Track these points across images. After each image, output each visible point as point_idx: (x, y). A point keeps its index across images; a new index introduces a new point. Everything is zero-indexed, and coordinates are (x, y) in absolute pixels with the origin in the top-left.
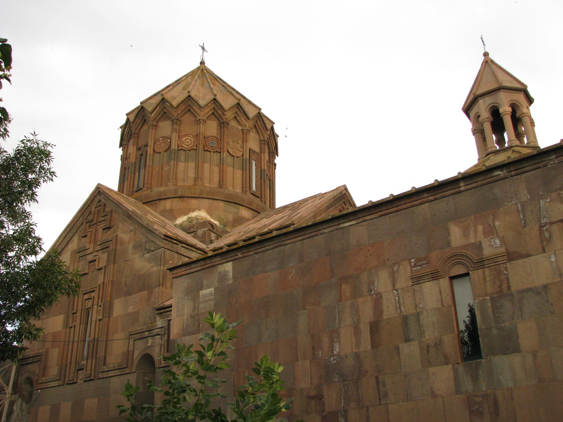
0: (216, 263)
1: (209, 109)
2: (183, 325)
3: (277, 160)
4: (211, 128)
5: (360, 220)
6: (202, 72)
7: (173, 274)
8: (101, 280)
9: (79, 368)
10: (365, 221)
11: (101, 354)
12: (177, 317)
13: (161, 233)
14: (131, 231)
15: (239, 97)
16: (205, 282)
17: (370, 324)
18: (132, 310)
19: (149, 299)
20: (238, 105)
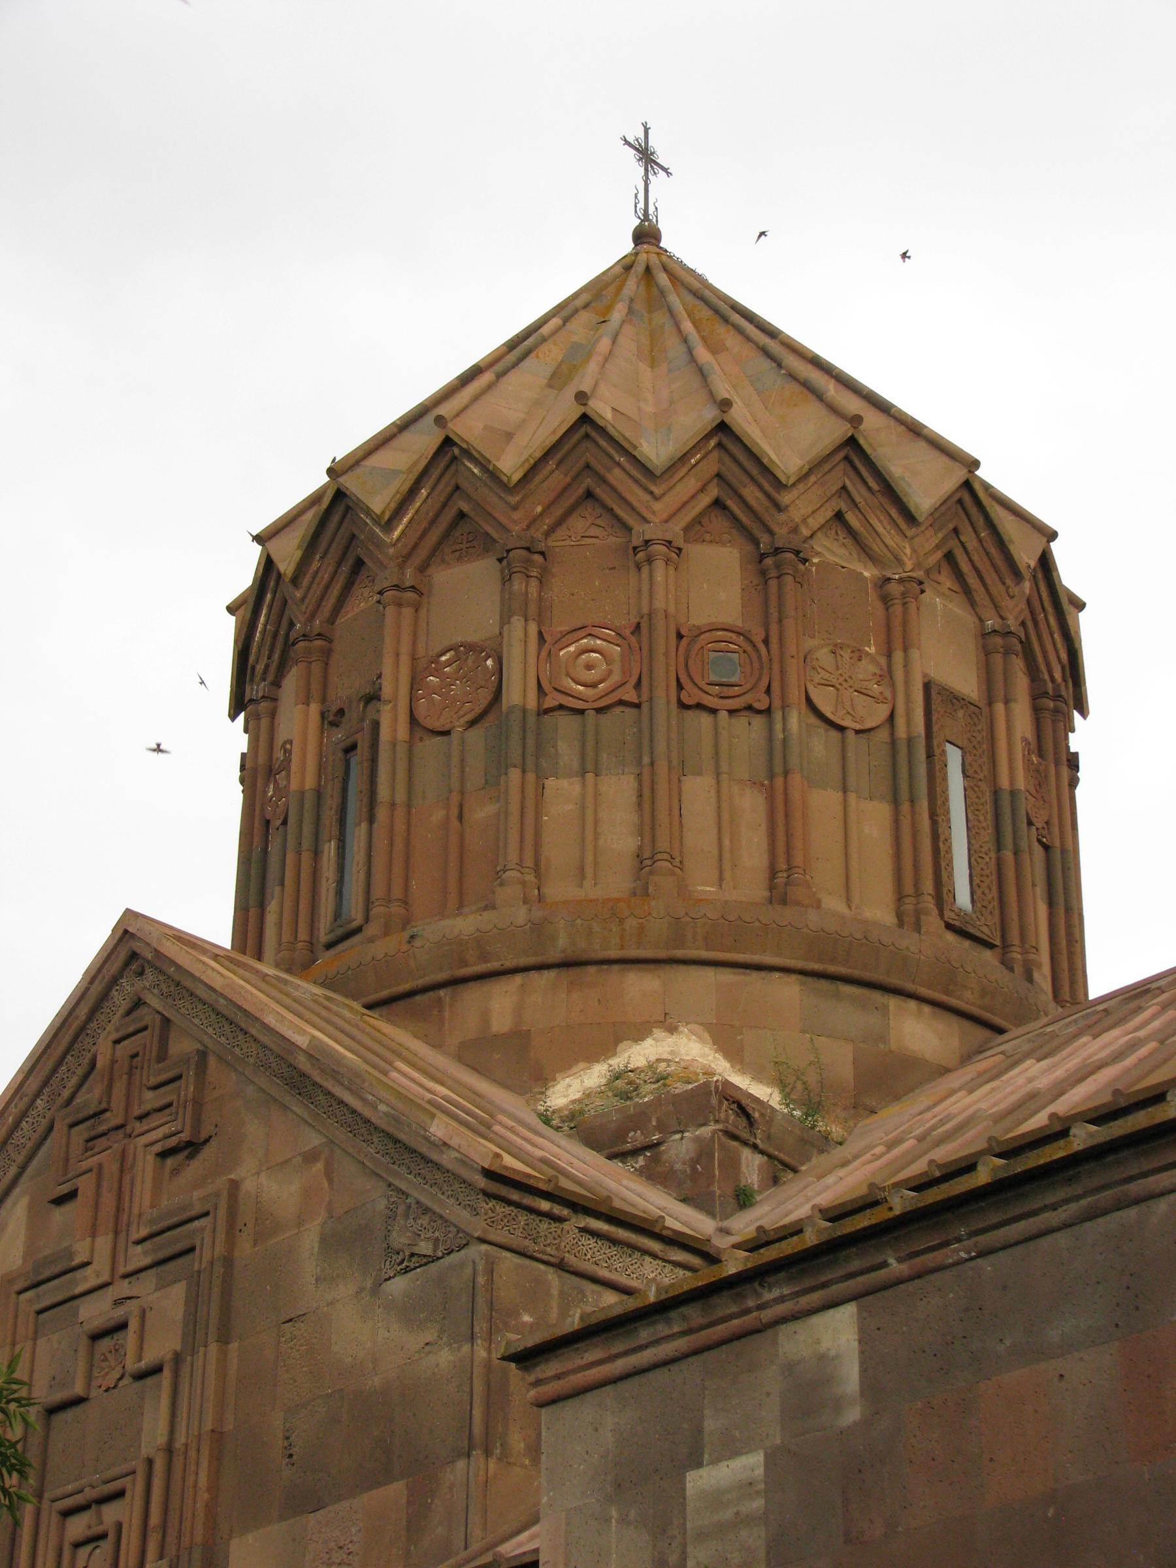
0: (767, 1315)
1: (692, 484)
3: (1083, 737)
6: (649, 284)
7: (538, 1383)
8: (154, 1430)
13: (465, 1161)
14: (311, 1157)
15: (853, 405)
16: (711, 1424)
19: (415, 1524)
20: (852, 450)
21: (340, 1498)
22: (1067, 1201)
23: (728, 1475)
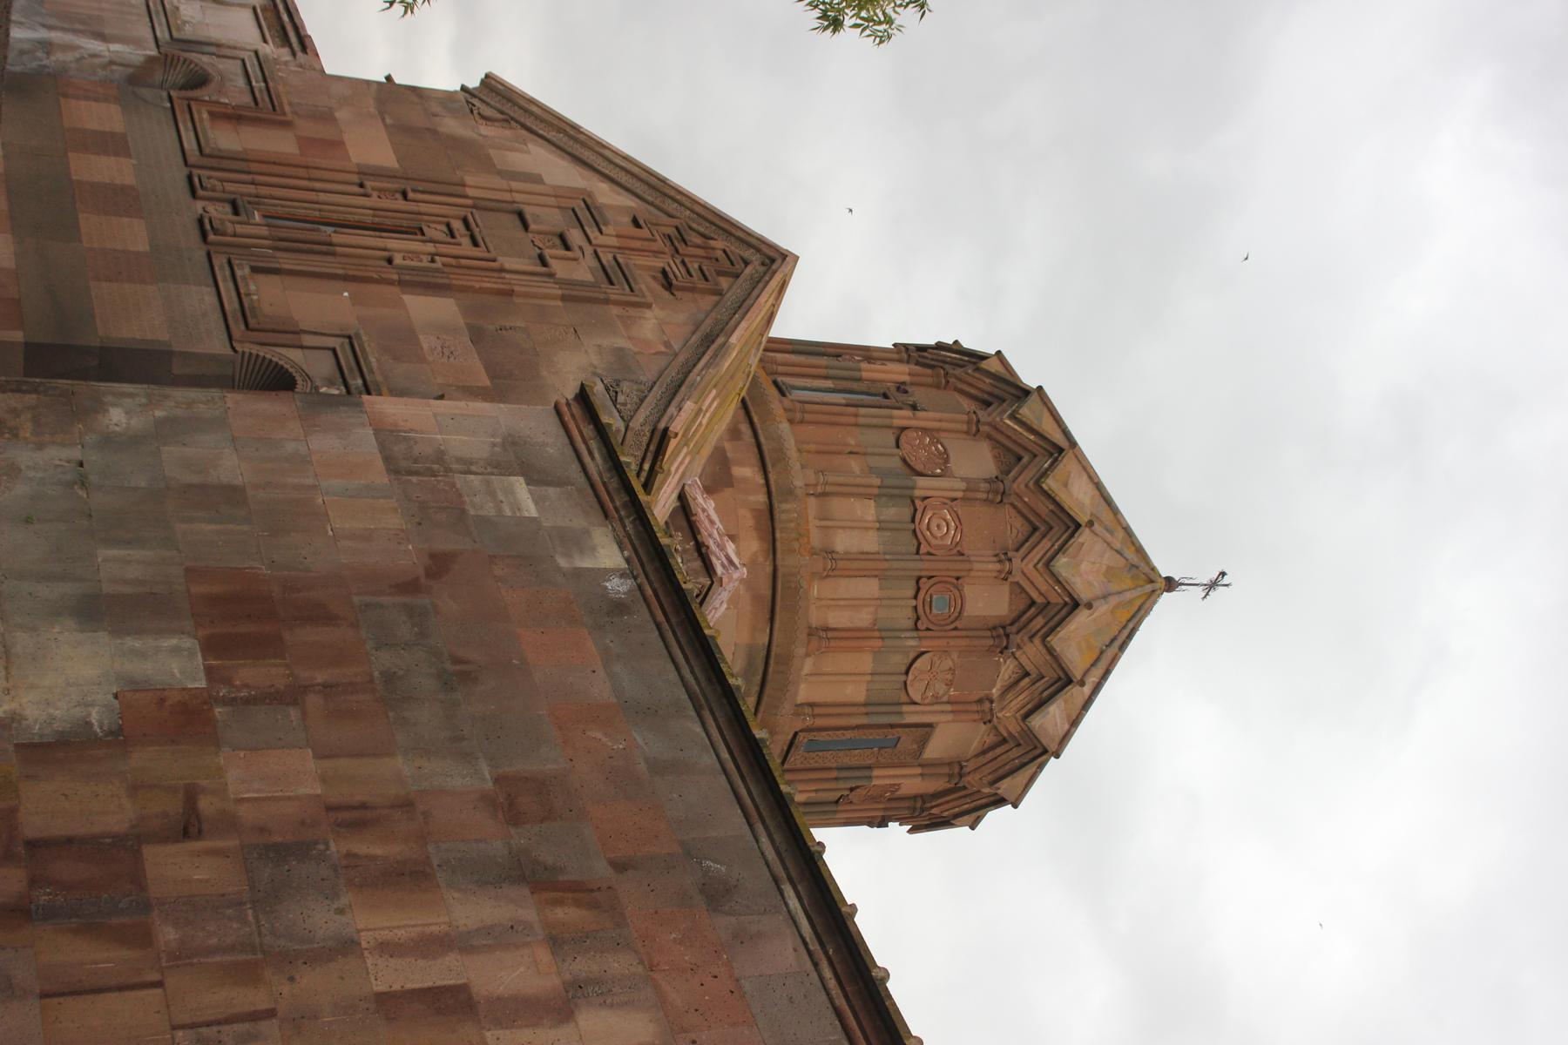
1: (1043, 587)
2: (411, 431)
4: (987, 601)
5: (814, 946)
7: (568, 404)
8: (511, 263)
9: (240, 202)
10: (816, 965)
11: (287, 261)
12: (435, 415)
13: (672, 418)
14: (667, 344)
15: (1091, 680)
17: (464, 988)
18: (425, 346)
21: (479, 353)
22: (696, 679)
23: (523, 498)
